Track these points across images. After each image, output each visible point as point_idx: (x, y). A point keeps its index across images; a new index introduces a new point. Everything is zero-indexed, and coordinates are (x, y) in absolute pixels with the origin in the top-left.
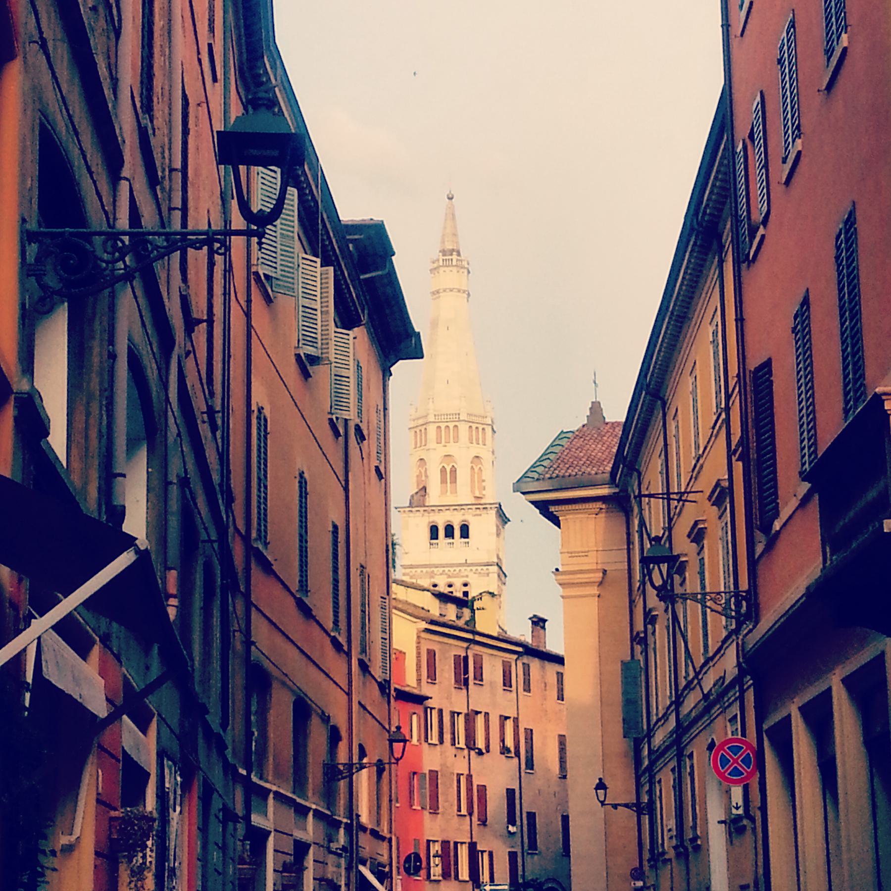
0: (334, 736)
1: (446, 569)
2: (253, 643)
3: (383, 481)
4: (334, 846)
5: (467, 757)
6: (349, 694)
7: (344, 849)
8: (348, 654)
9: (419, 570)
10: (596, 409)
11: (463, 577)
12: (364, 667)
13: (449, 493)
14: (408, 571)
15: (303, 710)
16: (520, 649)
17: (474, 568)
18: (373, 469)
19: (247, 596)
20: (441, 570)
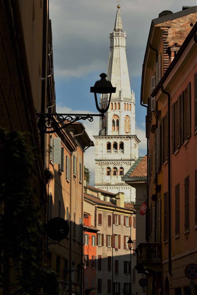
0: (66, 261)
3: (81, 184)
5: (112, 251)
6: (70, 250)
8: (70, 239)
11: (120, 165)
12: (74, 240)
14: (98, 162)
15: (58, 258)
16: (132, 212)
18: (78, 182)
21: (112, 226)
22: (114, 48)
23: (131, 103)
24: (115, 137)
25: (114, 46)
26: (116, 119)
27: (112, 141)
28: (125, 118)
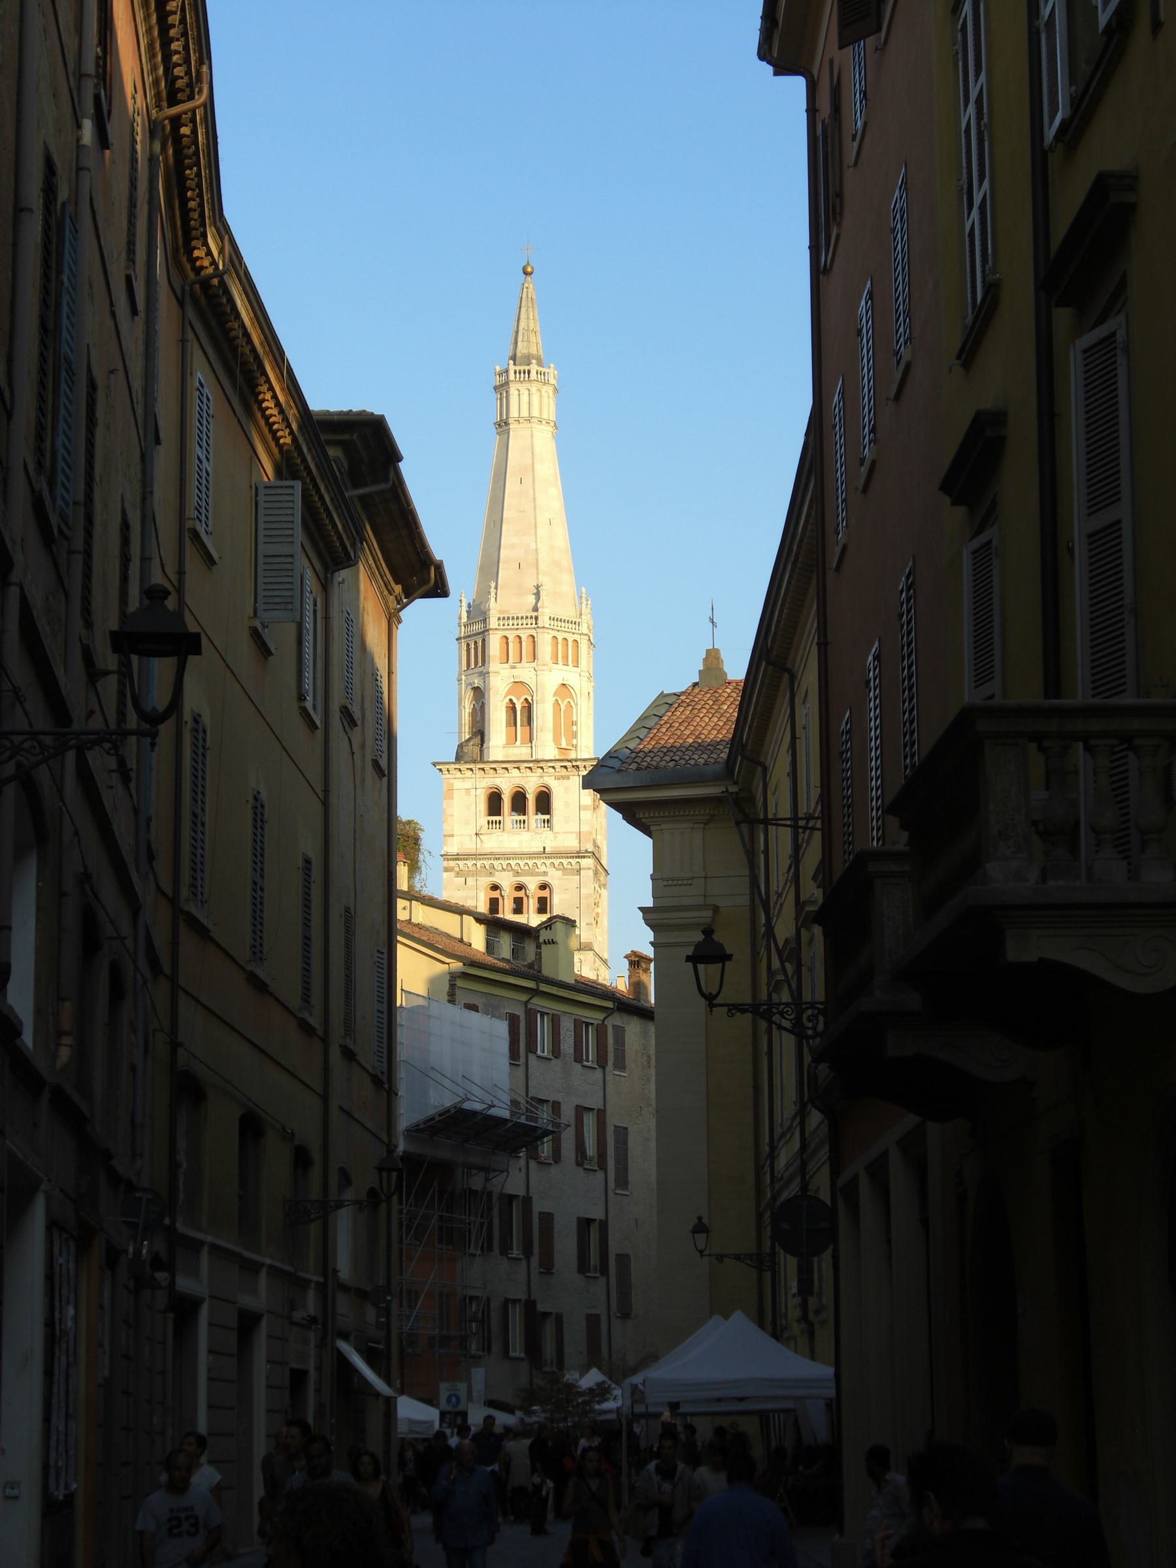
0: (302, 1158)
1: (513, 863)
2: (180, 1045)
3: (386, 779)
4: (298, 1315)
5: (524, 1170)
6: (325, 1098)
7: (313, 1320)
8: (325, 1041)
9: (470, 863)
10: (712, 660)
11: (538, 874)
12: (349, 1055)
13: (518, 743)
14: (452, 864)
15: (251, 1127)
16: (610, 1005)
17: (557, 862)
18: (369, 764)
19: (173, 979)
20: (504, 863)
21: (522, 1059)
22: (511, 426)
23: (577, 637)
24: (517, 763)
25: (511, 421)
26: (522, 699)
27: (507, 784)
28: (555, 695)
